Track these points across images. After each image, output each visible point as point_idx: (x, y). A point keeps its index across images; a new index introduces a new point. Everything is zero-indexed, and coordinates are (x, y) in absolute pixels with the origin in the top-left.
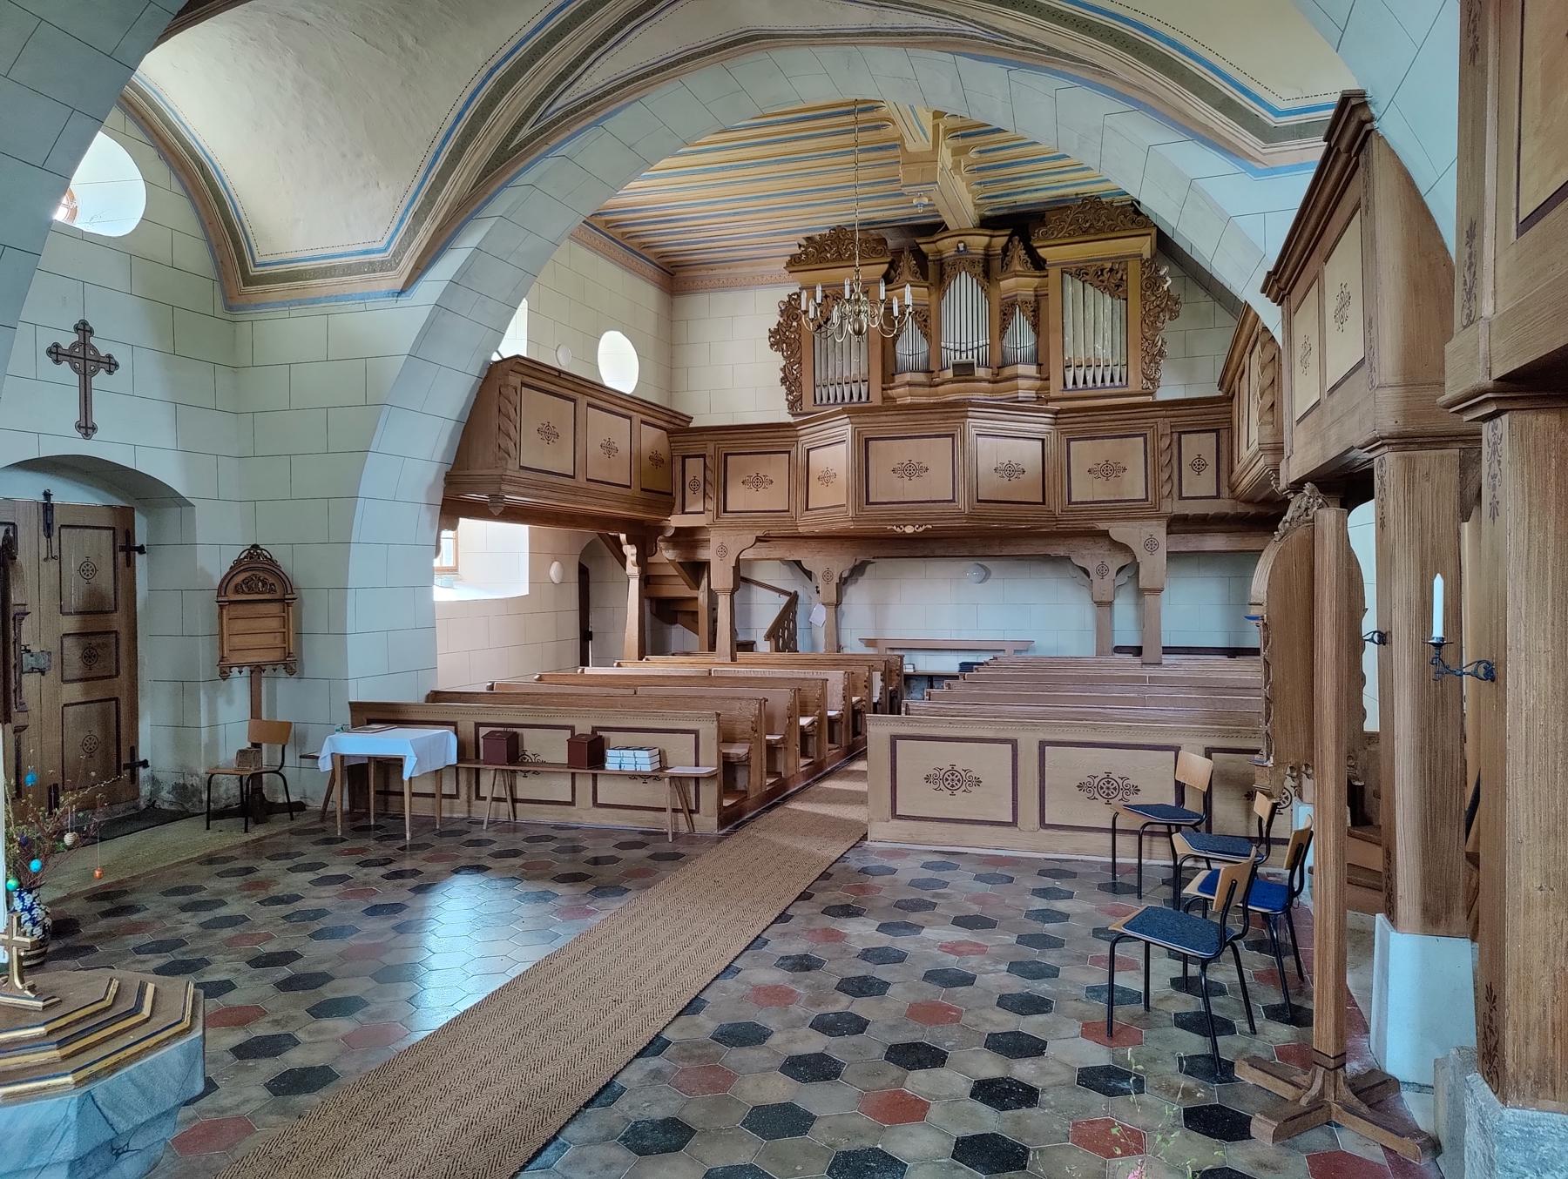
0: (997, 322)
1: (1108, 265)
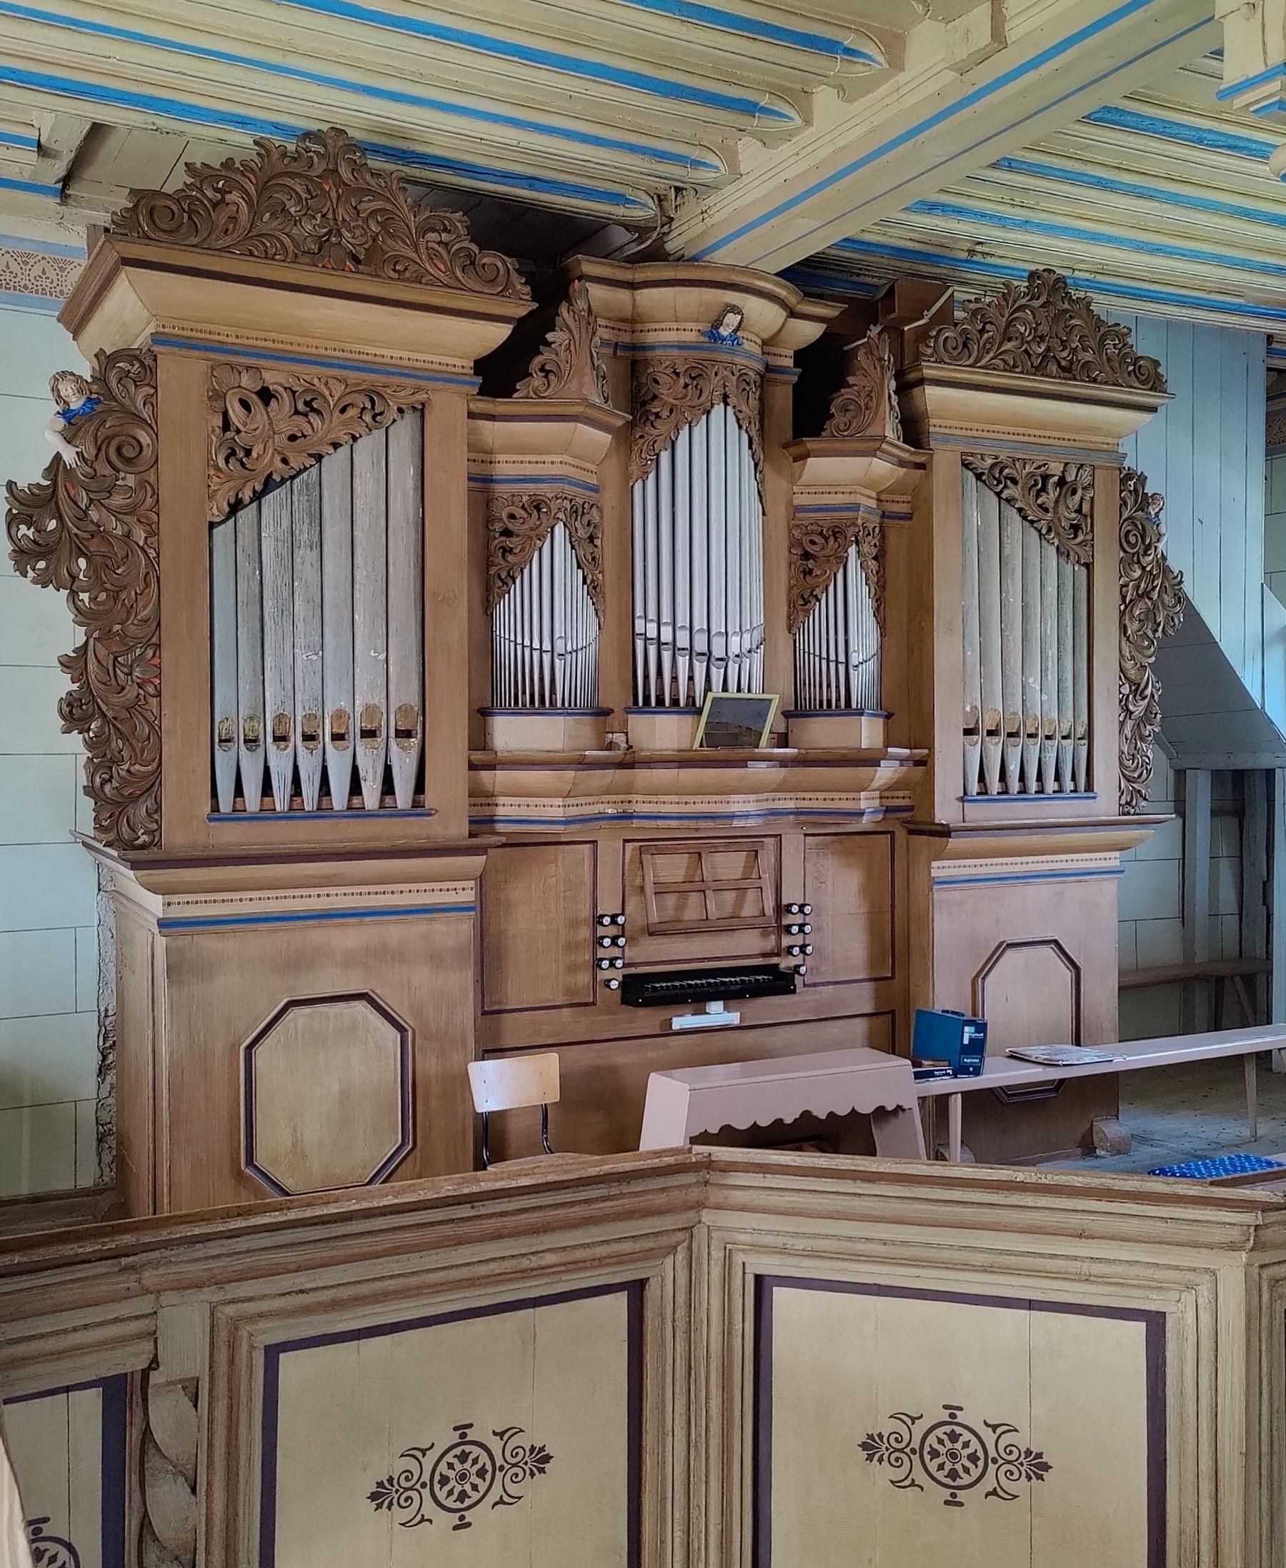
1: (1056, 468)
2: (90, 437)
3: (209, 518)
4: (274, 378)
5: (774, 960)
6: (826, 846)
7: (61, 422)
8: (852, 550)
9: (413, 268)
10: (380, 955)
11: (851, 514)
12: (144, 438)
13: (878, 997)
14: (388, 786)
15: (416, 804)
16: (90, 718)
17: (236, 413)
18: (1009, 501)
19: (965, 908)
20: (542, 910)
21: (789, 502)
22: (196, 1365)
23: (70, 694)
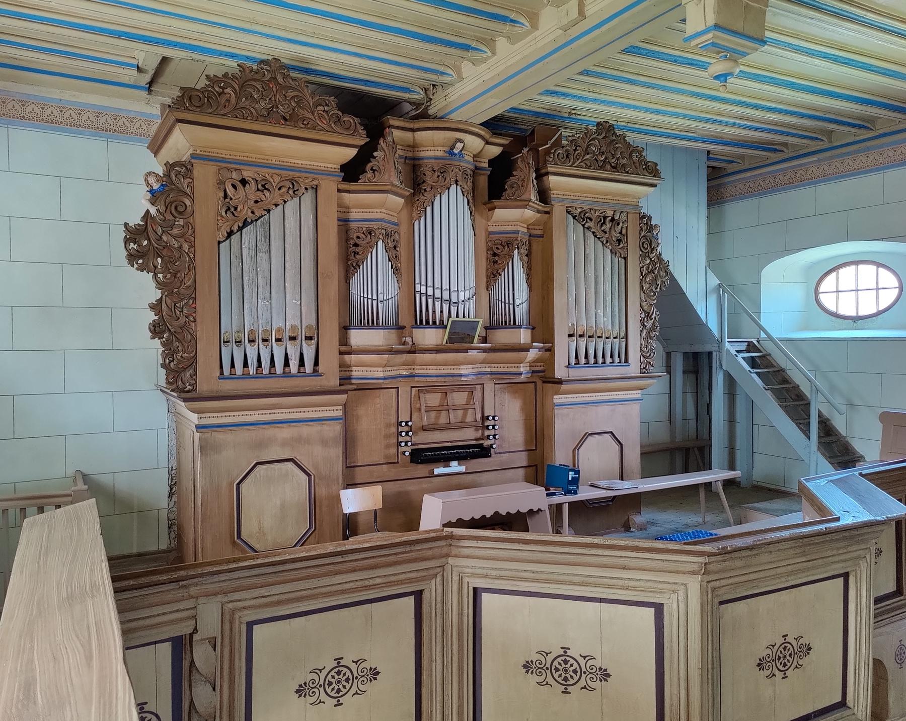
0: (483, 264)
1: (610, 213)
2: (162, 202)
3: (218, 239)
4: (247, 174)
5: (481, 442)
6: (505, 389)
7: (149, 195)
8: (516, 252)
9: (312, 122)
10: (300, 440)
11: (515, 235)
12: (188, 202)
13: (529, 458)
14: (302, 363)
15: (315, 371)
16: (164, 332)
17: (230, 191)
18: (588, 228)
19: (569, 417)
20: (374, 420)
21: (487, 230)
22: (215, 631)
23: (154, 321)
